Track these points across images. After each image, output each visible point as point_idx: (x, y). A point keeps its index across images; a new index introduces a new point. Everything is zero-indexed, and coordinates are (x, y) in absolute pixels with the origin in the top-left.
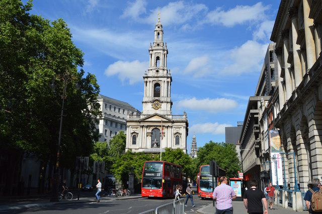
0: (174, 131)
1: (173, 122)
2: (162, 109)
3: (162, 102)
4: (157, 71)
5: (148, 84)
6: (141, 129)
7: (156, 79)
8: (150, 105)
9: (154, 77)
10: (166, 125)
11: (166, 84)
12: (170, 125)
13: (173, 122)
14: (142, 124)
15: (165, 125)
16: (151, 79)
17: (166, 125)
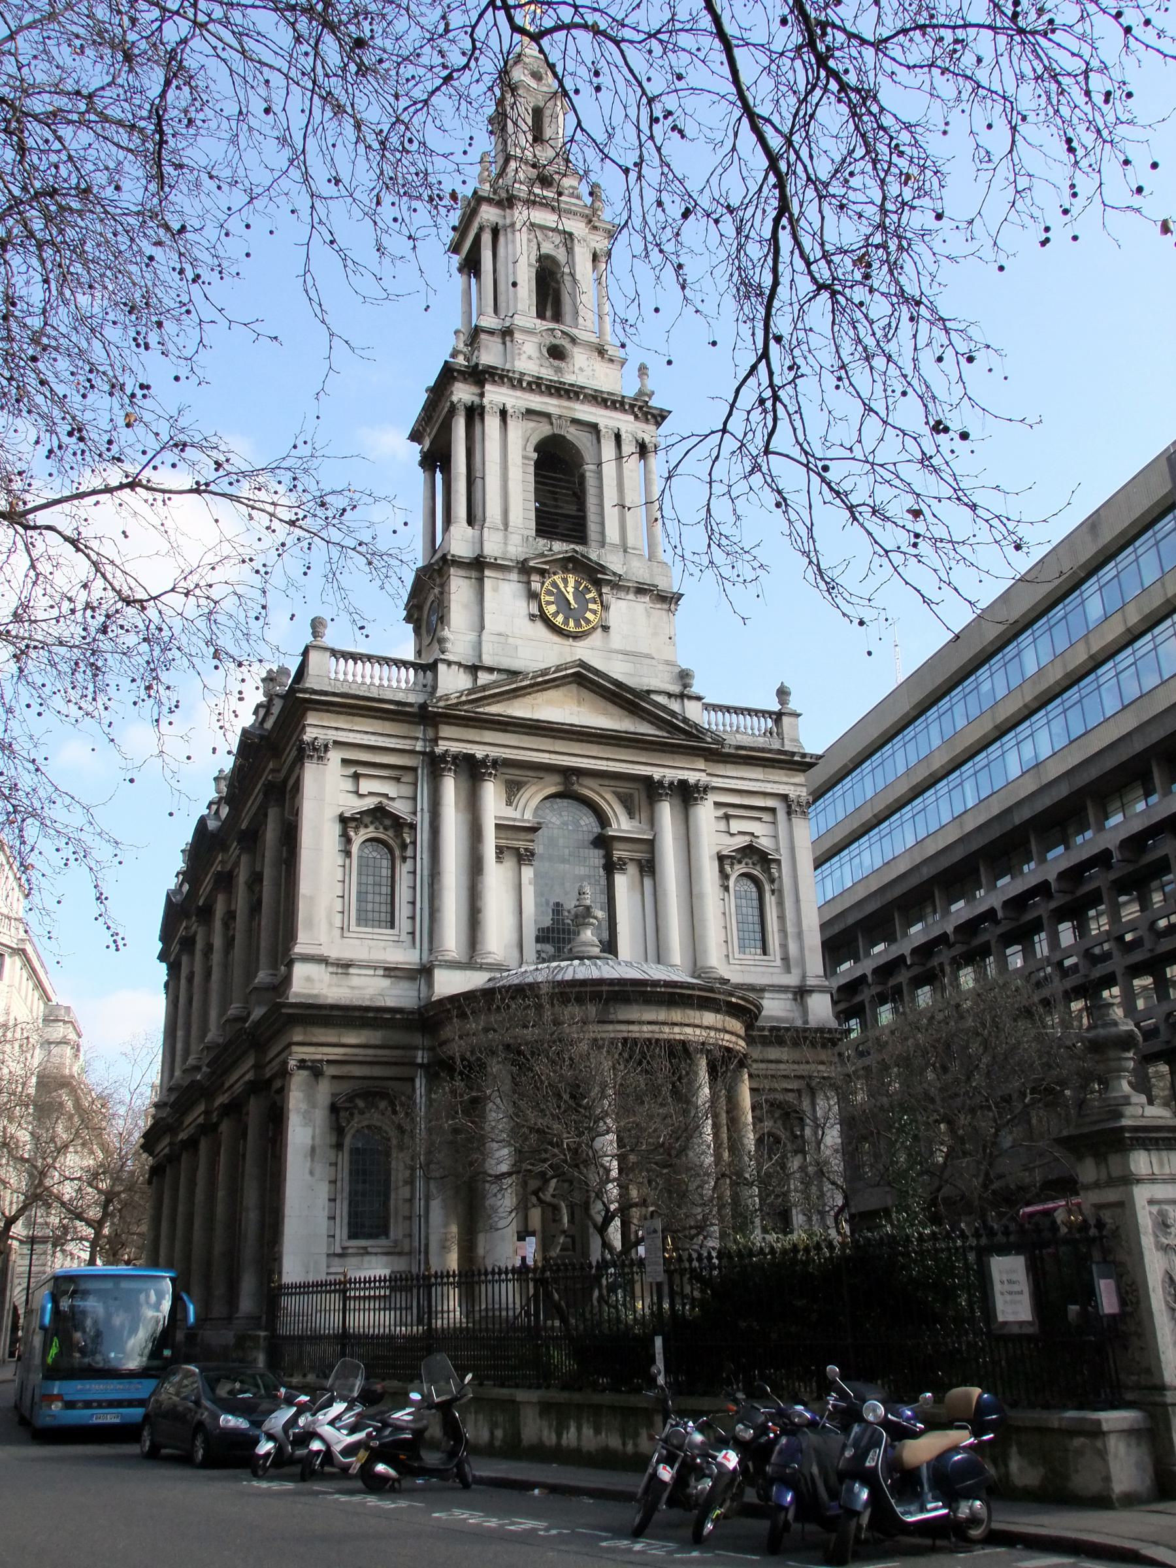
0: (712, 831)
1: (714, 752)
2: (616, 639)
3: (617, 585)
4: (556, 353)
5: (492, 423)
6: (450, 787)
7: (551, 405)
8: (505, 599)
9: (537, 385)
10: (667, 771)
11: (629, 447)
12: (692, 777)
13: (714, 752)
14: (452, 741)
15: (657, 773)
16: (514, 400)
17: (667, 771)
